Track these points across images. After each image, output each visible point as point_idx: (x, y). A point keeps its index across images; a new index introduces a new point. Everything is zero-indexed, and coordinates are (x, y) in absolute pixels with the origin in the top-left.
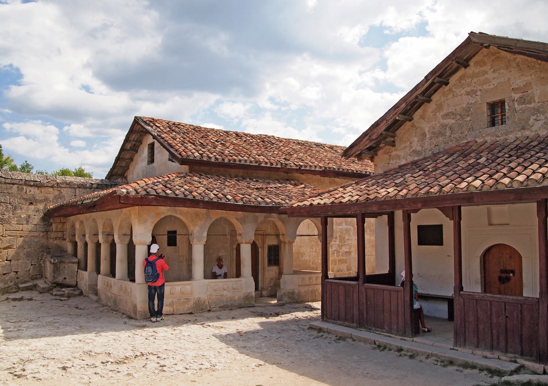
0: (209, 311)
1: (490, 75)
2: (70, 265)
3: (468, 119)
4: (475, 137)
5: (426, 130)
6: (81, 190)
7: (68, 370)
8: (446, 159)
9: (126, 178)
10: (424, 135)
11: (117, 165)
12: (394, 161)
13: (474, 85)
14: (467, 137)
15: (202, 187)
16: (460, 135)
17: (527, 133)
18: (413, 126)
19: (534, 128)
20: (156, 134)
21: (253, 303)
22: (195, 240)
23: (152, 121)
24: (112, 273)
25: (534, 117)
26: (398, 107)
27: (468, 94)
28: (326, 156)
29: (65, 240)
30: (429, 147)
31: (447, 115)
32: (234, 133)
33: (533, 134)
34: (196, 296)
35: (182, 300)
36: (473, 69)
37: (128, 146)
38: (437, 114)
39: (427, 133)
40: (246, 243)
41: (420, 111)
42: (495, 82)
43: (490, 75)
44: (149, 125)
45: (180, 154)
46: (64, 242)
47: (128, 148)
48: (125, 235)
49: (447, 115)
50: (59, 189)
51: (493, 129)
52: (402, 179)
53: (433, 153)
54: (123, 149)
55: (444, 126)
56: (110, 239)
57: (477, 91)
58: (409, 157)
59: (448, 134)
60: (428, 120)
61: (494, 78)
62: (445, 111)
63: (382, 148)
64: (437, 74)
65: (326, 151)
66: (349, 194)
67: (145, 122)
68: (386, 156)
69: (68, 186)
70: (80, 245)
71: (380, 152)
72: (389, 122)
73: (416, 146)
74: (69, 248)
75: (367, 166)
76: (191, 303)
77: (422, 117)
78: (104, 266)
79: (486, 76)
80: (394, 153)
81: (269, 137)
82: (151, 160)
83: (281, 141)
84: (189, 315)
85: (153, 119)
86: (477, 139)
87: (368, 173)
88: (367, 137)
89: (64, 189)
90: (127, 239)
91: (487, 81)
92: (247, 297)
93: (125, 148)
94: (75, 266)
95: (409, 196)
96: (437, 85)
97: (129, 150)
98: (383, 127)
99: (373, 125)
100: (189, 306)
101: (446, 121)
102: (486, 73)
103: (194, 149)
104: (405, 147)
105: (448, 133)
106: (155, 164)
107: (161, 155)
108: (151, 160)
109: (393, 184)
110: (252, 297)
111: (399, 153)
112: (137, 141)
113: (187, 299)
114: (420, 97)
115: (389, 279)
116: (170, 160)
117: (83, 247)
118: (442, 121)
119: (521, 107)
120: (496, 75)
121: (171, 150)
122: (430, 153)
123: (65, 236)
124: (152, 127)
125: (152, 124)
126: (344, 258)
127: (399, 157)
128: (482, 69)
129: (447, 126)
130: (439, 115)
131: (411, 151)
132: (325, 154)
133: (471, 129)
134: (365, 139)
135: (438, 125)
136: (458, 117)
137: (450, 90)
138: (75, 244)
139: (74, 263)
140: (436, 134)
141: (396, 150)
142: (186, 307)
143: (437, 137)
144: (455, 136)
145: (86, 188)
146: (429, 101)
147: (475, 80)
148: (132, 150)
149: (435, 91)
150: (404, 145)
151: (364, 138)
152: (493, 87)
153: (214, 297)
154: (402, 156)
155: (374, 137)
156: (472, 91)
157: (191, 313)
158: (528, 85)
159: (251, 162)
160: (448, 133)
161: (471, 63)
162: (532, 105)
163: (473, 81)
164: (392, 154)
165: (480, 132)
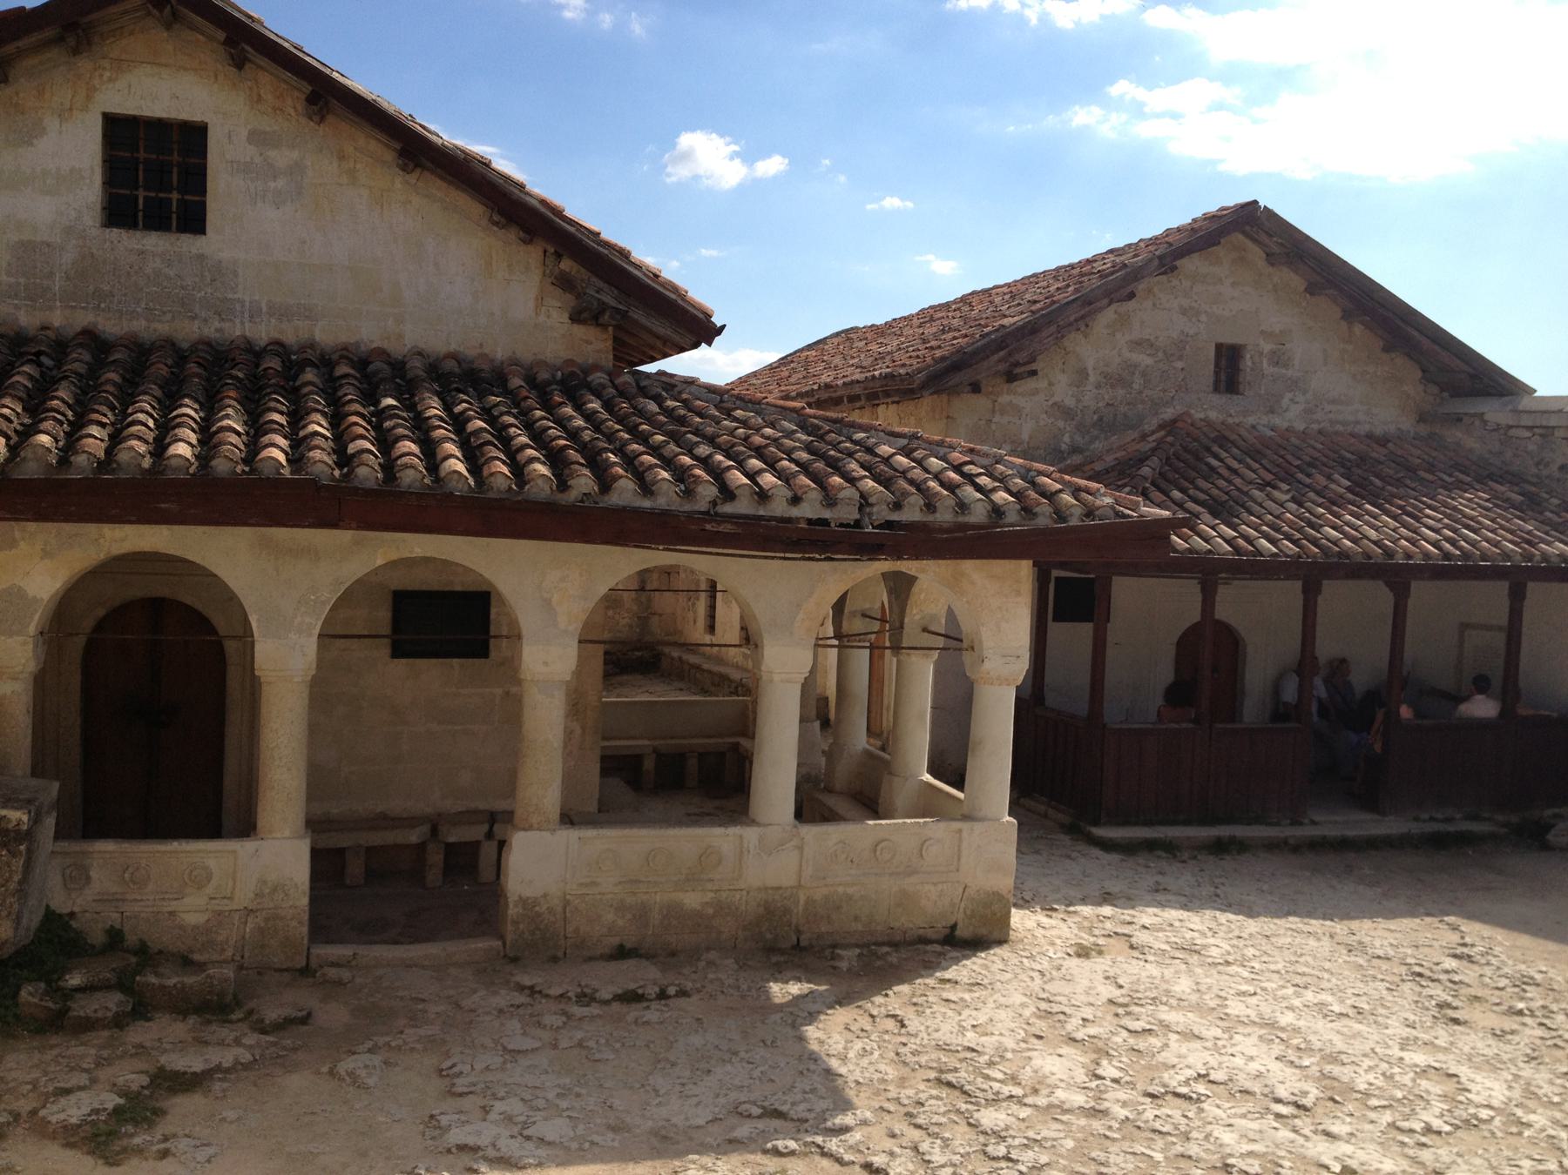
3: (1179, 365)
5: (1090, 364)
10: (1083, 374)
17: (1276, 421)
25: (1289, 395)
26: (1090, 303)
27: (1184, 311)
33: (1286, 425)
38: (1118, 335)
49: (1138, 344)
53: (1101, 419)
55: (1131, 367)
59: (1136, 386)
73: (1063, 392)
88: (1002, 353)
111: (1020, 401)
118: (1127, 354)
119: (1272, 369)
136: (1160, 354)
140: (1114, 380)
143: (1112, 386)
162: (1290, 373)
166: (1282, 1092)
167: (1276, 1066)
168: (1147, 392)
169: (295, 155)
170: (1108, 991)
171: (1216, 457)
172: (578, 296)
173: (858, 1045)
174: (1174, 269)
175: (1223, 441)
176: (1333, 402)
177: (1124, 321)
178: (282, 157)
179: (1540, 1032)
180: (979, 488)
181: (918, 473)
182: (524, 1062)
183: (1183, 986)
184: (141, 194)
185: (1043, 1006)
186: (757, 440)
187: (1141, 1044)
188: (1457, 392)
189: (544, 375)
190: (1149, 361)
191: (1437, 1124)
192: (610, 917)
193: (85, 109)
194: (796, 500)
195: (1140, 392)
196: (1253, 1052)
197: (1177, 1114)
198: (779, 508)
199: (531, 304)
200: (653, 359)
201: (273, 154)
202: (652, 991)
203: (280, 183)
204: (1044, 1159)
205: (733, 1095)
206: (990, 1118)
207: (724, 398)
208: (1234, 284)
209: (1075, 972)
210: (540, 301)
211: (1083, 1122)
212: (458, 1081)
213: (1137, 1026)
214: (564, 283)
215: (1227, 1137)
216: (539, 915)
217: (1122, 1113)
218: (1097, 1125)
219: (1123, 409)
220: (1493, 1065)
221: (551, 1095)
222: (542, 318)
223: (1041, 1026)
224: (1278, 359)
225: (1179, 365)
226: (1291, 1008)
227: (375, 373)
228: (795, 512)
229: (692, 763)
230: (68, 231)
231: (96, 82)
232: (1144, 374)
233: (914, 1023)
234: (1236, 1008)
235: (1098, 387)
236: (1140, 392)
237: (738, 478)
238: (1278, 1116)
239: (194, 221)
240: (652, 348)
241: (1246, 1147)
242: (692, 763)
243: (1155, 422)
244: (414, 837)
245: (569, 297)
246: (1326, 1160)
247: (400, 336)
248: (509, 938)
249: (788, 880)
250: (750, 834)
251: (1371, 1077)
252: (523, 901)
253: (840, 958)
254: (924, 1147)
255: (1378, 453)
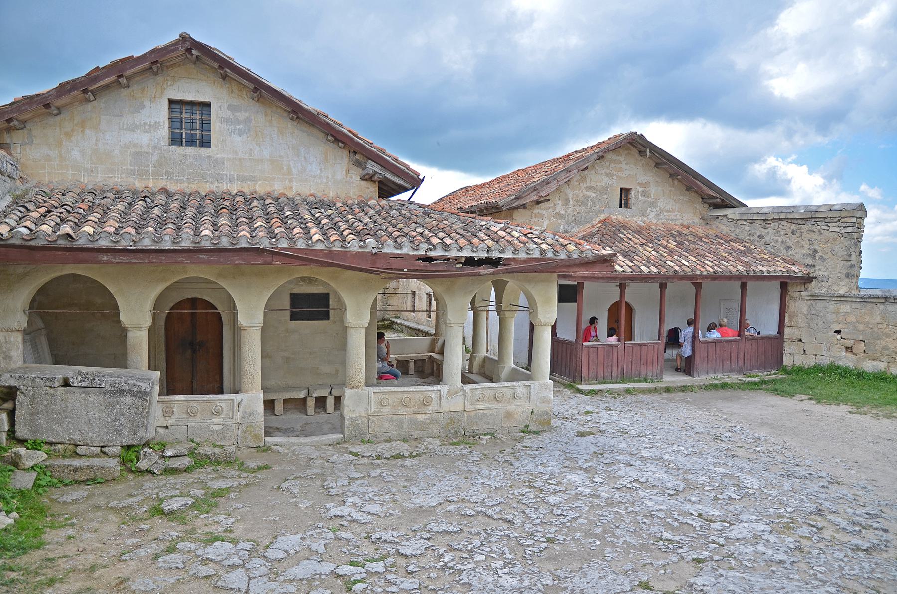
1: (624, 166)
3: (606, 197)
5: (570, 196)
10: (567, 200)
19: (650, 217)
31: (589, 188)
42: (627, 173)
62: (588, 184)
91: (621, 170)
101: (588, 194)
111: (543, 212)
120: (627, 167)
129: (589, 197)
130: (583, 186)
147: (612, 165)
158: (648, 183)
166: (669, 485)
167: (665, 475)
169: (247, 114)
170: (592, 449)
171: (623, 233)
172: (363, 170)
173: (495, 473)
174: (603, 157)
175: (625, 227)
176: (668, 211)
178: (242, 115)
179: (767, 459)
180: (535, 243)
181: (510, 239)
182: (358, 482)
183: (623, 445)
184: (184, 131)
185: (568, 455)
186: (441, 226)
187: (610, 469)
188: (716, 206)
189: (350, 202)
191: (734, 496)
192: (387, 425)
193: (161, 97)
194: (461, 249)
196: (654, 470)
197: (628, 495)
198: (454, 253)
199: (344, 173)
200: (393, 195)
201: (238, 114)
202: (407, 454)
203: (241, 126)
204: (577, 515)
205: (446, 494)
206: (552, 499)
207: (427, 211)
209: (579, 441)
210: (348, 171)
211: (590, 500)
212: (331, 490)
213: (607, 462)
214: (358, 164)
215: (650, 504)
216: (358, 424)
217: (606, 495)
218: (597, 501)
220: (751, 472)
221: (370, 495)
222: (348, 179)
223: (567, 463)
224: (645, 194)
225: (606, 197)
226: (668, 453)
227: (282, 202)
228: (460, 254)
229: (412, 365)
230: (155, 147)
231: (165, 86)
232: (592, 201)
233: (516, 464)
234: (645, 454)
237: (435, 241)
238: (669, 495)
239: (205, 143)
240: (393, 190)
241: (658, 508)
242: (412, 365)
243: (597, 220)
244: (302, 395)
245: (360, 170)
246: (691, 511)
247: (291, 188)
248: (347, 433)
249: (460, 408)
250: (444, 389)
251: (704, 478)
252: (351, 418)
253: (482, 439)
254: (527, 512)
255: (686, 231)
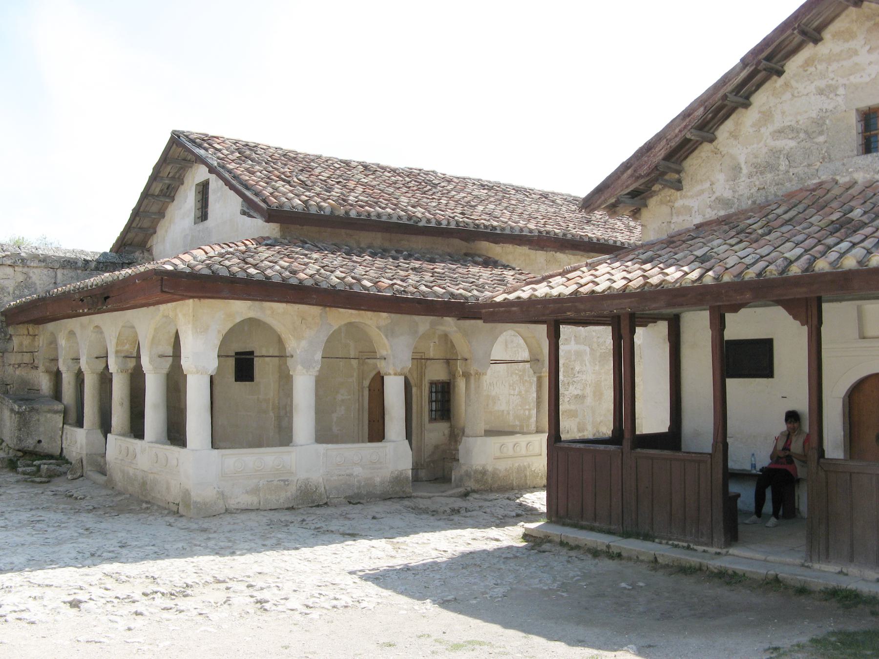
0: (326, 504)
1: (863, 57)
2: (49, 415)
3: (821, 139)
4: (835, 174)
5: (742, 159)
6: (66, 272)
7: (82, 606)
8: (786, 212)
9: (149, 250)
10: (737, 169)
11: (134, 225)
12: (681, 218)
13: (831, 75)
14: (820, 174)
15: (310, 265)
16: (806, 170)
18: (716, 152)
20: (216, 164)
21: (409, 490)
22: (299, 367)
23: (206, 141)
24: (137, 430)
26: (689, 115)
27: (821, 92)
28: (537, 211)
29: (37, 368)
30: (747, 193)
32: (360, 163)
34: (302, 475)
35: (275, 483)
36: (829, 45)
37: (157, 189)
38: (763, 130)
39: (743, 166)
40: (395, 374)
41: (729, 124)
43: (863, 57)
44: (200, 146)
45: (264, 201)
46: (34, 372)
47: (157, 192)
48: (161, 356)
49: (780, 132)
50: (25, 270)
51: (869, 157)
52: (706, 249)
53: (754, 202)
54: (146, 195)
55: (775, 153)
56: (132, 364)
57: (837, 88)
58: (709, 210)
59: (783, 168)
60: (745, 140)
61: (870, 63)
62: (778, 124)
63: (655, 193)
64: (764, 54)
65: (536, 202)
66: (609, 277)
67: (193, 141)
68: (665, 209)
69: (43, 264)
70: (68, 380)
71: (653, 202)
72: (673, 144)
74: (45, 383)
75: (622, 230)
76: (292, 490)
77: (734, 135)
78: (119, 416)
79: (855, 59)
80: (679, 203)
81: (427, 173)
82: (203, 215)
83: (449, 181)
84: (288, 512)
85: (207, 135)
86: (838, 178)
87: (618, 244)
88: (629, 172)
89: (35, 270)
90: (167, 363)
92: (398, 480)
93: (151, 192)
94: (59, 418)
95: (726, 278)
96: (763, 73)
97: (158, 196)
98: (660, 153)
99: (641, 149)
100: (289, 494)
102: (856, 52)
103: (291, 192)
104: (702, 192)
105: (783, 165)
106: (210, 222)
107: (225, 204)
108: (203, 215)
109: (692, 258)
110: (407, 478)
111: (688, 202)
112: (173, 178)
113: (284, 481)
114: (731, 97)
115: (671, 439)
116: (244, 213)
117: (73, 383)
118: (772, 143)
121: (248, 193)
122: (750, 202)
123: (36, 361)
124: (206, 150)
125: (206, 145)
126: (573, 407)
127: (688, 210)
128: (846, 46)
129: (780, 151)
130: (766, 131)
131: (713, 198)
132: (535, 206)
133: (827, 158)
134: (625, 175)
135: (765, 150)
136: (802, 135)
137: (787, 85)
138: (57, 376)
139: (56, 412)
140: (761, 169)
141: (685, 197)
142: (284, 496)
143: (762, 173)
144: (796, 171)
145: (76, 269)
146: (747, 105)
147: (834, 66)
148: (165, 195)
149: (759, 86)
150: (698, 188)
151: (623, 172)
152: (867, 79)
153: (335, 478)
154: (696, 208)
155: (643, 171)
156: (829, 86)
157: (293, 508)
159: (400, 217)
160: (783, 165)
161: (827, 34)
163: (830, 69)
164: (676, 205)
165: (844, 164)
168: (792, 171)
177: (767, 116)
190: (792, 144)
195: (788, 172)
208: (870, 51)
219: (773, 189)
235: (750, 176)
236: (788, 172)
